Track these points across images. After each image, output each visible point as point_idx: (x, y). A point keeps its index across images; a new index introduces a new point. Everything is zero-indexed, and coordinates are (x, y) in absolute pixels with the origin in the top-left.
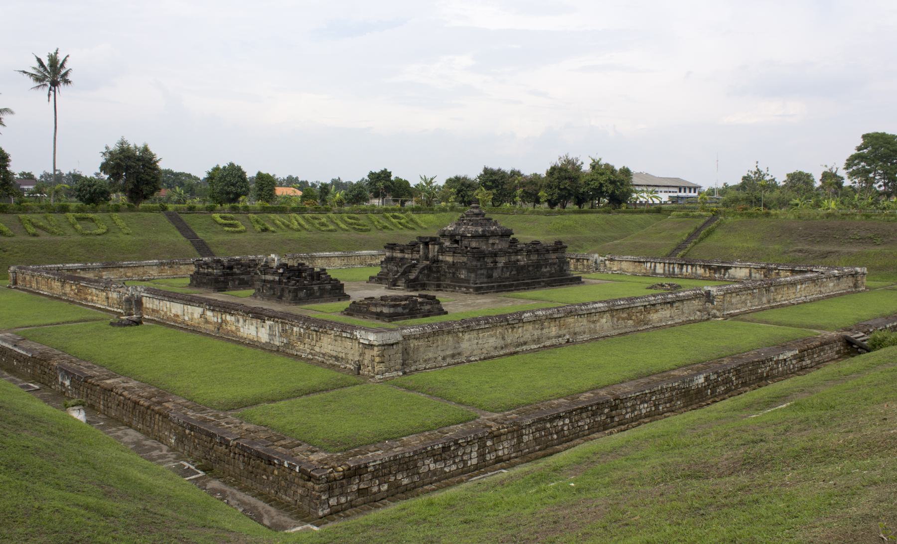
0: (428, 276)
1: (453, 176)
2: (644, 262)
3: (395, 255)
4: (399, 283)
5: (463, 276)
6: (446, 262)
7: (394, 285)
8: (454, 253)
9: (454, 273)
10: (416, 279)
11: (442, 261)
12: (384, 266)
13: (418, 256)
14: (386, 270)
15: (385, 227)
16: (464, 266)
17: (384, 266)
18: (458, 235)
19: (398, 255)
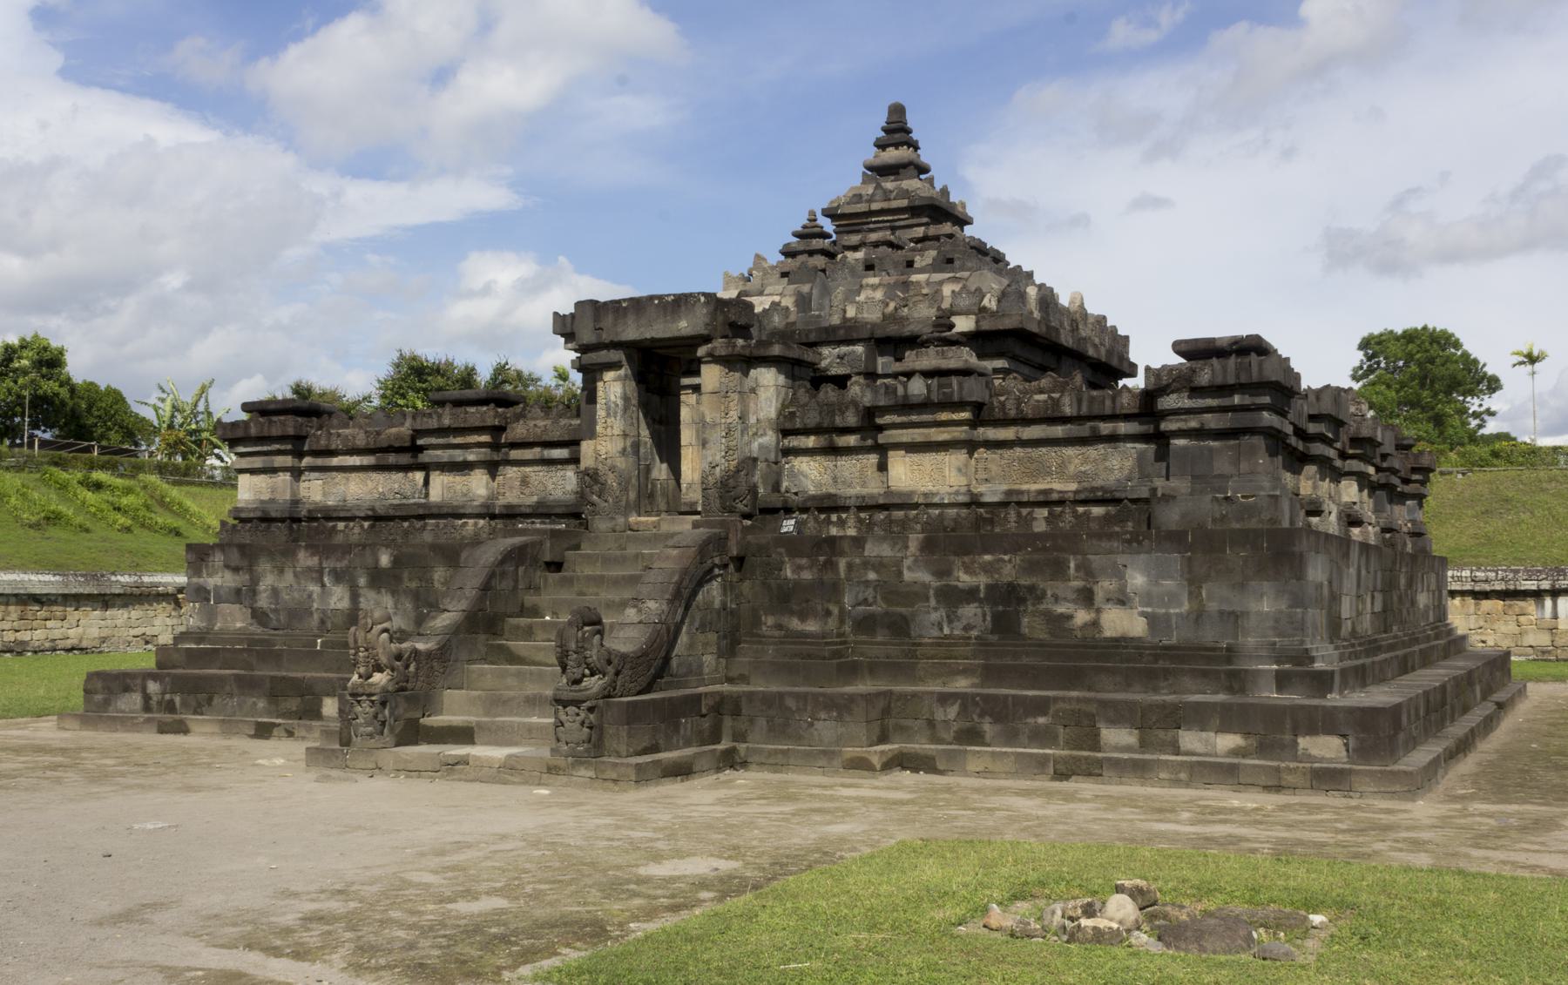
0: (733, 634)
1: (282, 391)
2: (1537, 595)
3: (315, 491)
4: (453, 709)
5: (1121, 622)
6: (889, 510)
7: (413, 734)
8: (981, 414)
9: (1007, 602)
10: (655, 663)
11: (828, 505)
12: (219, 579)
13: (561, 484)
14: (235, 619)
15: (54, 519)
16: (1129, 516)
17: (219, 579)
18: (844, 334)
19: (360, 488)
